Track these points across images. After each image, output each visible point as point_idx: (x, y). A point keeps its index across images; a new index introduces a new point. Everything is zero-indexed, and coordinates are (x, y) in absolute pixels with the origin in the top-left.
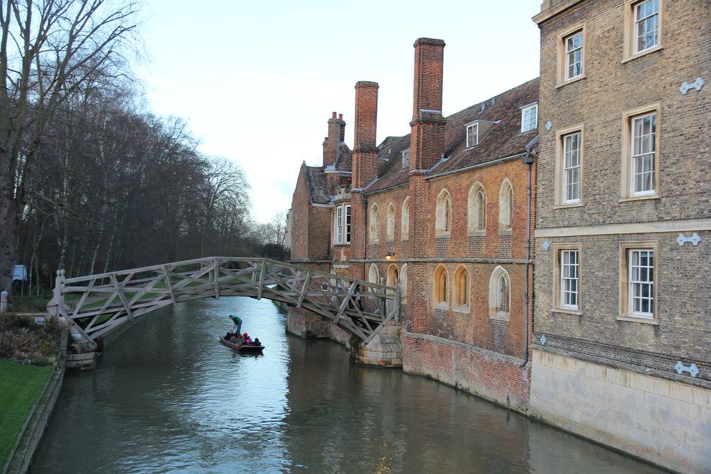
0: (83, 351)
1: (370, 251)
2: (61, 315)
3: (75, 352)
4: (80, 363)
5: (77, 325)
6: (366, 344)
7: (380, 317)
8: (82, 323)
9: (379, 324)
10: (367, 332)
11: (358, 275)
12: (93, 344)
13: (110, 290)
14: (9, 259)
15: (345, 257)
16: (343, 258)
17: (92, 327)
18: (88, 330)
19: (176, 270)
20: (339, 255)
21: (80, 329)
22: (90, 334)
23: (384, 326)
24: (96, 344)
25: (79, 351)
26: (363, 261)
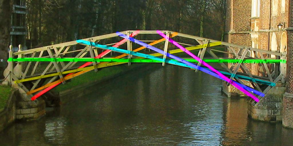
0: (29, 107)
1: (272, 22)
2: (13, 80)
3: (21, 108)
4: (26, 116)
5: (24, 87)
6: (256, 103)
7: (269, 80)
8: (28, 85)
9: (268, 86)
10: (257, 92)
11: (265, 43)
12: (36, 101)
13: (48, 60)
14: (4, 38)
15: (258, 27)
16: (256, 29)
17: (36, 88)
18: (33, 91)
19: (102, 42)
20: (254, 27)
21: (27, 90)
22: (34, 94)
23: (271, 87)
24: (38, 102)
25: (25, 107)
26: (267, 31)
